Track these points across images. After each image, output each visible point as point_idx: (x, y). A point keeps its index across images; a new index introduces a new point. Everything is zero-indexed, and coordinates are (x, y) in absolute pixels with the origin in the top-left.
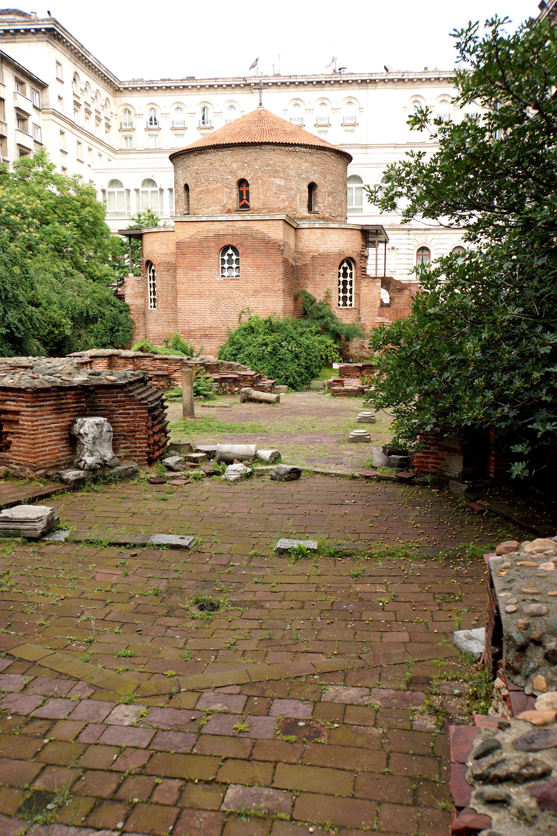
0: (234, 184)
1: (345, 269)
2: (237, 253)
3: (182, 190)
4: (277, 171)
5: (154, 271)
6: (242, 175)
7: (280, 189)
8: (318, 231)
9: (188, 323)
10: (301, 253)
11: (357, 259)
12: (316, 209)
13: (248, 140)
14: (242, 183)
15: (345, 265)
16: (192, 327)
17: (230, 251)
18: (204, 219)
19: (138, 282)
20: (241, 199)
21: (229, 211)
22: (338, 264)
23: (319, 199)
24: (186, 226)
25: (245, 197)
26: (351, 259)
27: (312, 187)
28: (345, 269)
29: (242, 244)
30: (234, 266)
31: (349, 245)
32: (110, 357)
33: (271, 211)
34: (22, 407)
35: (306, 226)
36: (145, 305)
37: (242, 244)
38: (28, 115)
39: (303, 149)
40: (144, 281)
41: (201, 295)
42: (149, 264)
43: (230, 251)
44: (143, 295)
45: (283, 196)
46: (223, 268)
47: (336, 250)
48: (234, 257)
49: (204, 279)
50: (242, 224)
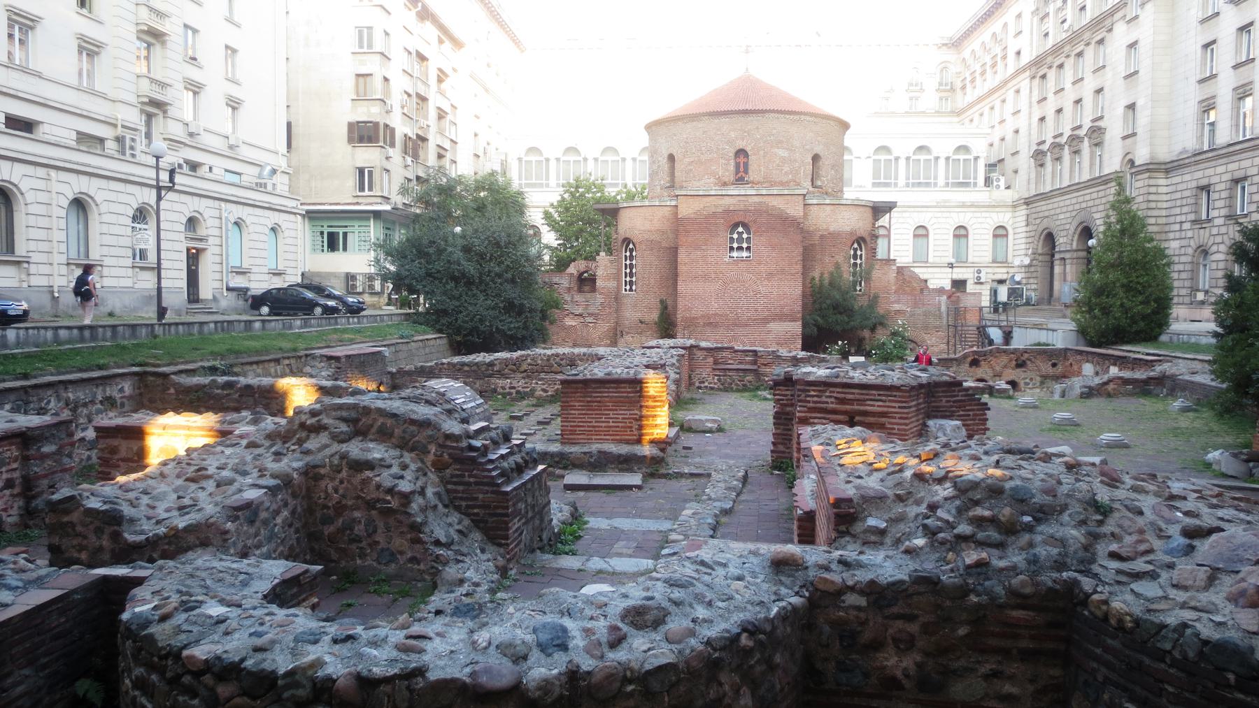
0: (732, 155)
1: (855, 250)
2: (749, 233)
3: (664, 161)
4: (781, 142)
5: (631, 251)
6: (741, 144)
7: (783, 160)
8: (828, 208)
9: (690, 309)
10: (808, 232)
11: (868, 239)
12: (819, 183)
13: (748, 107)
14: (741, 153)
15: (856, 246)
16: (694, 313)
17: (740, 229)
18: (713, 193)
19: (611, 262)
20: (737, 172)
21: (725, 184)
22: (849, 243)
23: (823, 173)
24: (691, 200)
25: (742, 169)
26: (863, 239)
27: (816, 158)
28: (855, 250)
29: (755, 222)
30: (745, 245)
31: (861, 224)
32: (692, 346)
33: (772, 184)
34: (894, 407)
35: (815, 202)
36: (619, 288)
37: (755, 222)
38: (447, 76)
39: (808, 118)
40: (618, 261)
41: (706, 277)
42: (627, 241)
43: (740, 229)
44: (617, 277)
45: (786, 169)
46: (732, 249)
47: (848, 229)
48: (745, 236)
49: (710, 259)
50: (756, 199)
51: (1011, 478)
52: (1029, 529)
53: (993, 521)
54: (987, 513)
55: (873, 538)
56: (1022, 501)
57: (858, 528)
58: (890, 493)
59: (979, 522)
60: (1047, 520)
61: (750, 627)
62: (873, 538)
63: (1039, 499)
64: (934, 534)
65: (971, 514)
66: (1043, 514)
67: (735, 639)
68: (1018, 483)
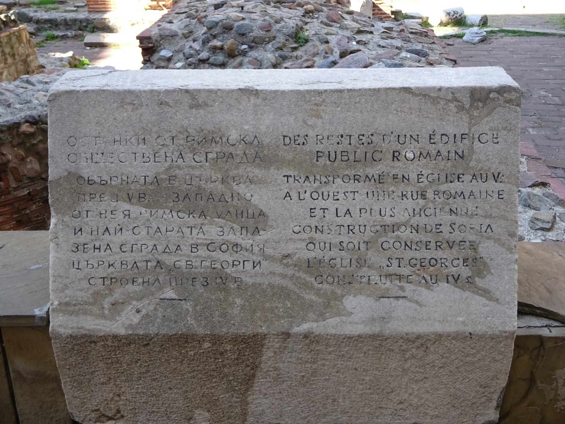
51: (243, 19)
52: (244, 53)
53: (222, 48)
54: (219, 44)
55: (163, 64)
56: (243, 35)
57: (155, 58)
58: (180, 32)
59: (214, 49)
60: (257, 47)
61: (30, 120)
62: (163, 64)
63: (257, 33)
64: (187, 59)
65: (210, 44)
66: (256, 43)
67: (17, 125)
68: (246, 22)
